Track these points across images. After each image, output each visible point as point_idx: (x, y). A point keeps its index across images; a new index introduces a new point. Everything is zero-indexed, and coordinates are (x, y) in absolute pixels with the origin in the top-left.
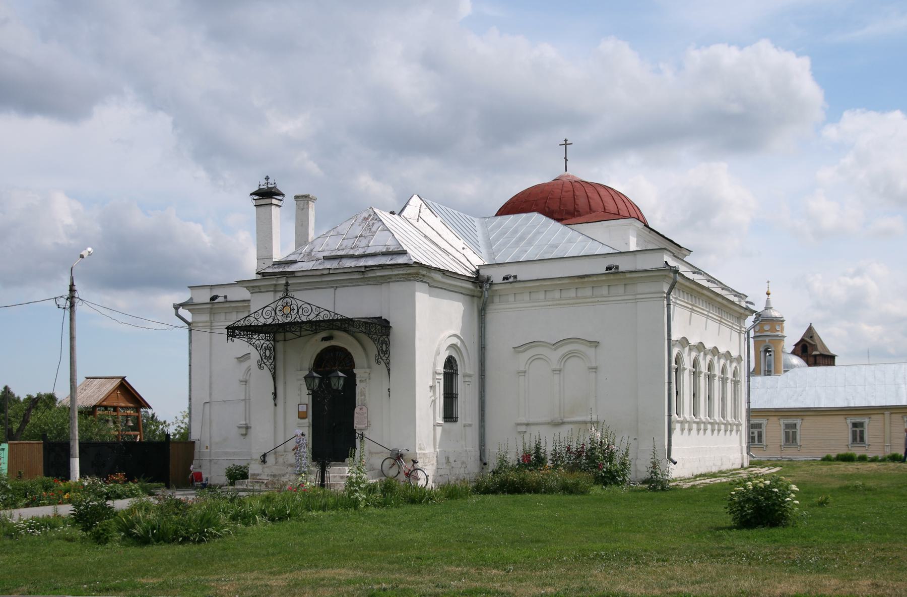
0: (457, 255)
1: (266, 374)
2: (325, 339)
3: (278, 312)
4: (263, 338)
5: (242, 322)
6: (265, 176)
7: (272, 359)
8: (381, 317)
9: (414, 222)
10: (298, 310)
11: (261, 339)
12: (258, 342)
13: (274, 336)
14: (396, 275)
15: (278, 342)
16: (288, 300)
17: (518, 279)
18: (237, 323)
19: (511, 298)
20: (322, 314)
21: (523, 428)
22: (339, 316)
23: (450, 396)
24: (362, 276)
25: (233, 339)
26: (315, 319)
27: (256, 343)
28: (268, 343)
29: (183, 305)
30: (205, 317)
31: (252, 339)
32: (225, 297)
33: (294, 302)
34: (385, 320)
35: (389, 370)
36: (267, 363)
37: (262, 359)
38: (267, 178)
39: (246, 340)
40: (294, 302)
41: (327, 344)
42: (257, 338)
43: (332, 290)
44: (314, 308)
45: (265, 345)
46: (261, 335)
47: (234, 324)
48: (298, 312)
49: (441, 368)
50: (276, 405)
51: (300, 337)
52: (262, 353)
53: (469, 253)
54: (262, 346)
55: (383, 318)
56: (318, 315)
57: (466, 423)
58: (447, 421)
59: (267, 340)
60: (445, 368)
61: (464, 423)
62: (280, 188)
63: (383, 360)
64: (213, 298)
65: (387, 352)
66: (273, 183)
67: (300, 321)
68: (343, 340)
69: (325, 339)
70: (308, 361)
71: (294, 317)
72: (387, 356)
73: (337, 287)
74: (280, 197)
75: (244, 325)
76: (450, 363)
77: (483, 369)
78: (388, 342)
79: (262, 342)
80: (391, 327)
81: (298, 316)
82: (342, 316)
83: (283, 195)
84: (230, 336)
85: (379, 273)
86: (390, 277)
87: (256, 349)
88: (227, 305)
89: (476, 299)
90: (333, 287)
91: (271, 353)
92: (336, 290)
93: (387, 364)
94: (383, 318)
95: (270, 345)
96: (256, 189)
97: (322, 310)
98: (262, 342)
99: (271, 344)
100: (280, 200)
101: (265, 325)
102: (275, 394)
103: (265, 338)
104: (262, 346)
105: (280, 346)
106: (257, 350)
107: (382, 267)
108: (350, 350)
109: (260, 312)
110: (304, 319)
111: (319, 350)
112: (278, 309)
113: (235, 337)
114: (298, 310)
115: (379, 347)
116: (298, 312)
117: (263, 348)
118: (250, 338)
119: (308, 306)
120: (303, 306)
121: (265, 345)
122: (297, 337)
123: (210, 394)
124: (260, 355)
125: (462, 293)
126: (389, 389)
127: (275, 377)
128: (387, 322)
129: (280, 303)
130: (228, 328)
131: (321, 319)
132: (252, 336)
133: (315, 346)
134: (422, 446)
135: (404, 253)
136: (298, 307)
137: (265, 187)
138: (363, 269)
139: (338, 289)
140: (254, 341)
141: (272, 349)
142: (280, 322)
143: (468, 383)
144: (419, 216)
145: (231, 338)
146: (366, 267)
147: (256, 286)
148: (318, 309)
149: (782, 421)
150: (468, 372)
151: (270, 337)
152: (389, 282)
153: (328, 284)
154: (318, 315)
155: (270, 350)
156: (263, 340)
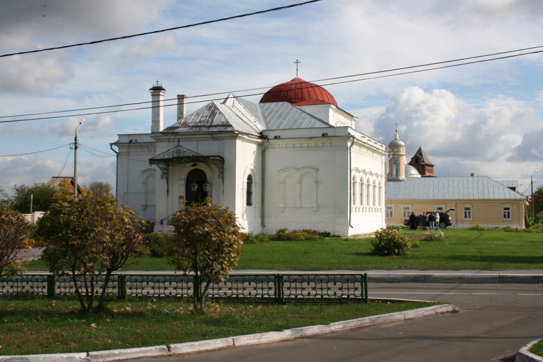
0: (252, 125)
1: (164, 181)
2: (193, 165)
3: (174, 153)
6: (156, 81)
9: (231, 108)
10: (184, 152)
12: (161, 166)
14: (227, 137)
15: (170, 166)
16: (179, 148)
23: (249, 193)
24: (211, 136)
28: (165, 166)
29: (115, 144)
30: (125, 150)
32: (136, 140)
35: (223, 181)
36: (165, 176)
38: (157, 82)
40: (182, 148)
41: (193, 168)
44: (192, 152)
48: (184, 153)
49: (246, 181)
50: (168, 196)
53: (257, 123)
62: (164, 87)
64: (131, 142)
65: (223, 173)
66: (160, 84)
68: (201, 166)
70: (184, 175)
73: (199, 141)
74: (163, 91)
76: (250, 178)
79: (163, 166)
83: (165, 90)
85: (220, 135)
86: (224, 137)
88: (137, 144)
89: (260, 147)
93: (223, 178)
96: (152, 87)
100: (164, 93)
101: (168, 159)
102: (168, 191)
105: (170, 168)
107: (220, 132)
108: (204, 170)
109: (166, 153)
111: (189, 170)
112: (174, 152)
113: (152, 164)
114: (184, 152)
116: (184, 153)
119: (189, 151)
120: (187, 151)
123: (127, 189)
128: (223, 158)
129: (175, 149)
133: (188, 168)
135: (231, 126)
137: (156, 86)
138: (211, 133)
139: (200, 142)
144: (233, 105)
146: (213, 132)
147: (159, 139)
149: (402, 206)
152: (224, 140)
155: (166, 170)
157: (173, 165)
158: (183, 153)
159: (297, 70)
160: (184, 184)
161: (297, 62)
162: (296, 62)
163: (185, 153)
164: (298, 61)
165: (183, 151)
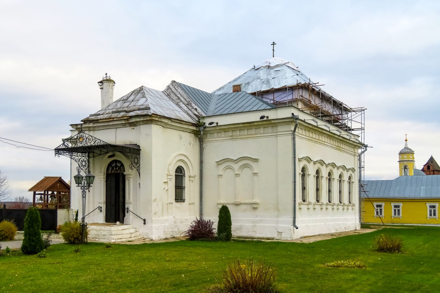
2: (110, 157)
4: (81, 155)
5: (62, 145)
7: (87, 166)
8: (137, 144)
10: (86, 139)
11: (79, 156)
12: (77, 157)
13: (88, 154)
15: (90, 157)
17: (219, 124)
18: (59, 147)
19: (216, 135)
20: (97, 142)
22: (105, 142)
25: (59, 155)
26: (93, 145)
28: (84, 158)
29: (67, 140)
31: (72, 156)
33: (84, 135)
34: (138, 145)
35: (139, 174)
36: (84, 169)
37: (79, 166)
39: (68, 156)
42: (76, 155)
43: (115, 129)
44: (93, 138)
45: (82, 159)
46: (79, 154)
47: (58, 147)
48: (86, 141)
49: (173, 173)
51: (100, 155)
52: (80, 163)
54: (79, 160)
55: (137, 145)
56: (95, 142)
57: (191, 202)
58: (177, 202)
59: (84, 157)
60: (176, 172)
61: (190, 202)
63: (135, 167)
67: (87, 145)
68: (119, 157)
69: (110, 157)
71: (84, 143)
72: (138, 165)
73: (117, 128)
75: (62, 148)
77: (201, 173)
78: (139, 158)
79: (80, 157)
80: (141, 149)
81: (86, 143)
82: (106, 143)
84: (57, 154)
87: (76, 161)
90: (115, 128)
91: (86, 164)
92: (117, 130)
94: (137, 145)
95: (86, 160)
97: (97, 139)
98: (80, 157)
99: (86, 159)
103: (82, 155)
104: (79, 160)
105: (91, 160)
106: (76, 162)
110: (89, 144)
114: (86, 139)
115: (132, 160)
116: (86, 141)
117: (80, 160)
119: (91, 137)
120: (89, 137)
121: (82, 159)
122: (99, 155)
124: (79, 165)
126: (139, 184)
128: (139, 146)
130: (55, 149)
131: (97, 144)
132: (72, 154)
136: (86, 137)
140: (74, 157)
141: (87, 161)
142: (78, 146)
143: (192, 181)
145: (57, 155)
148: (95, 139)
150: (192, 174)
151: (85, 155)
153: (113, 126)
154: (95, 142)
156: (80, 156)
157: (94, 157)
158: (85, 140)
160: (104, 178)
163: (87, 139)
165: (85, 138)
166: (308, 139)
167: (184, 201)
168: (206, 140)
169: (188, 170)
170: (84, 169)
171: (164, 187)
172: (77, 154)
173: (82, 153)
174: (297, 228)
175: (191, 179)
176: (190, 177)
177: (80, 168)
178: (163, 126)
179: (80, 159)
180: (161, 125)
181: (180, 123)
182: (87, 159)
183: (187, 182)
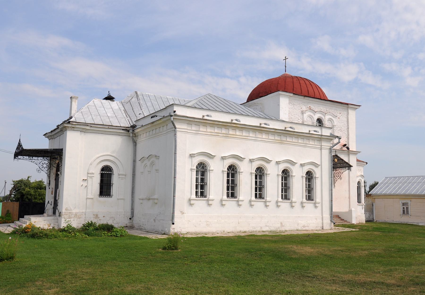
12: (37, 161)
21: (141, 201)
27: (36, 161)
36: (44, 170)
39: (28, 160)
52: (40, 165)
59: (45, 160)
61: (118, 197)
73: (60, 135)
118: (31, 159)
125: (125, 136)
127: (50, 176)
132: (32, 158)
134: (69, 209)
144: (130, 101)
159: (286, 67)
161: (286, 59)
162: (285, 59)
164: (286, 58)
166: (210, 135)
167: (111, 196)
168: (138, 141)
169: (118, 169)
170: (44, 170)
171: (82, 184)
172: (38, 158)
173: (29, 156)
174: (173, 224)
175: (120, 176)
176: (119, 175)
177: (40, 169)
178: (81, 131)
179: (41, 162)
180: (79, 131)
181: (108, 128)
182: (49, 162)
183: (115, 180)
